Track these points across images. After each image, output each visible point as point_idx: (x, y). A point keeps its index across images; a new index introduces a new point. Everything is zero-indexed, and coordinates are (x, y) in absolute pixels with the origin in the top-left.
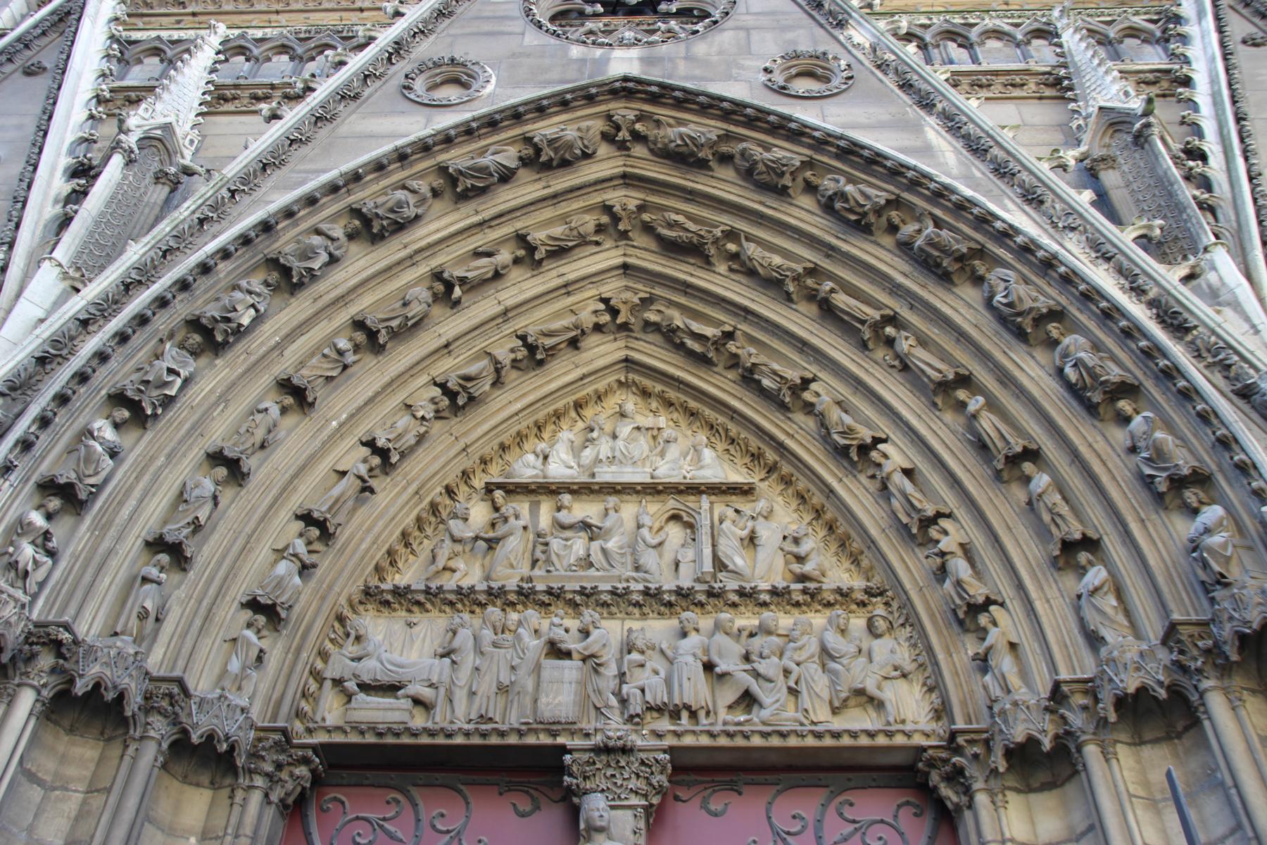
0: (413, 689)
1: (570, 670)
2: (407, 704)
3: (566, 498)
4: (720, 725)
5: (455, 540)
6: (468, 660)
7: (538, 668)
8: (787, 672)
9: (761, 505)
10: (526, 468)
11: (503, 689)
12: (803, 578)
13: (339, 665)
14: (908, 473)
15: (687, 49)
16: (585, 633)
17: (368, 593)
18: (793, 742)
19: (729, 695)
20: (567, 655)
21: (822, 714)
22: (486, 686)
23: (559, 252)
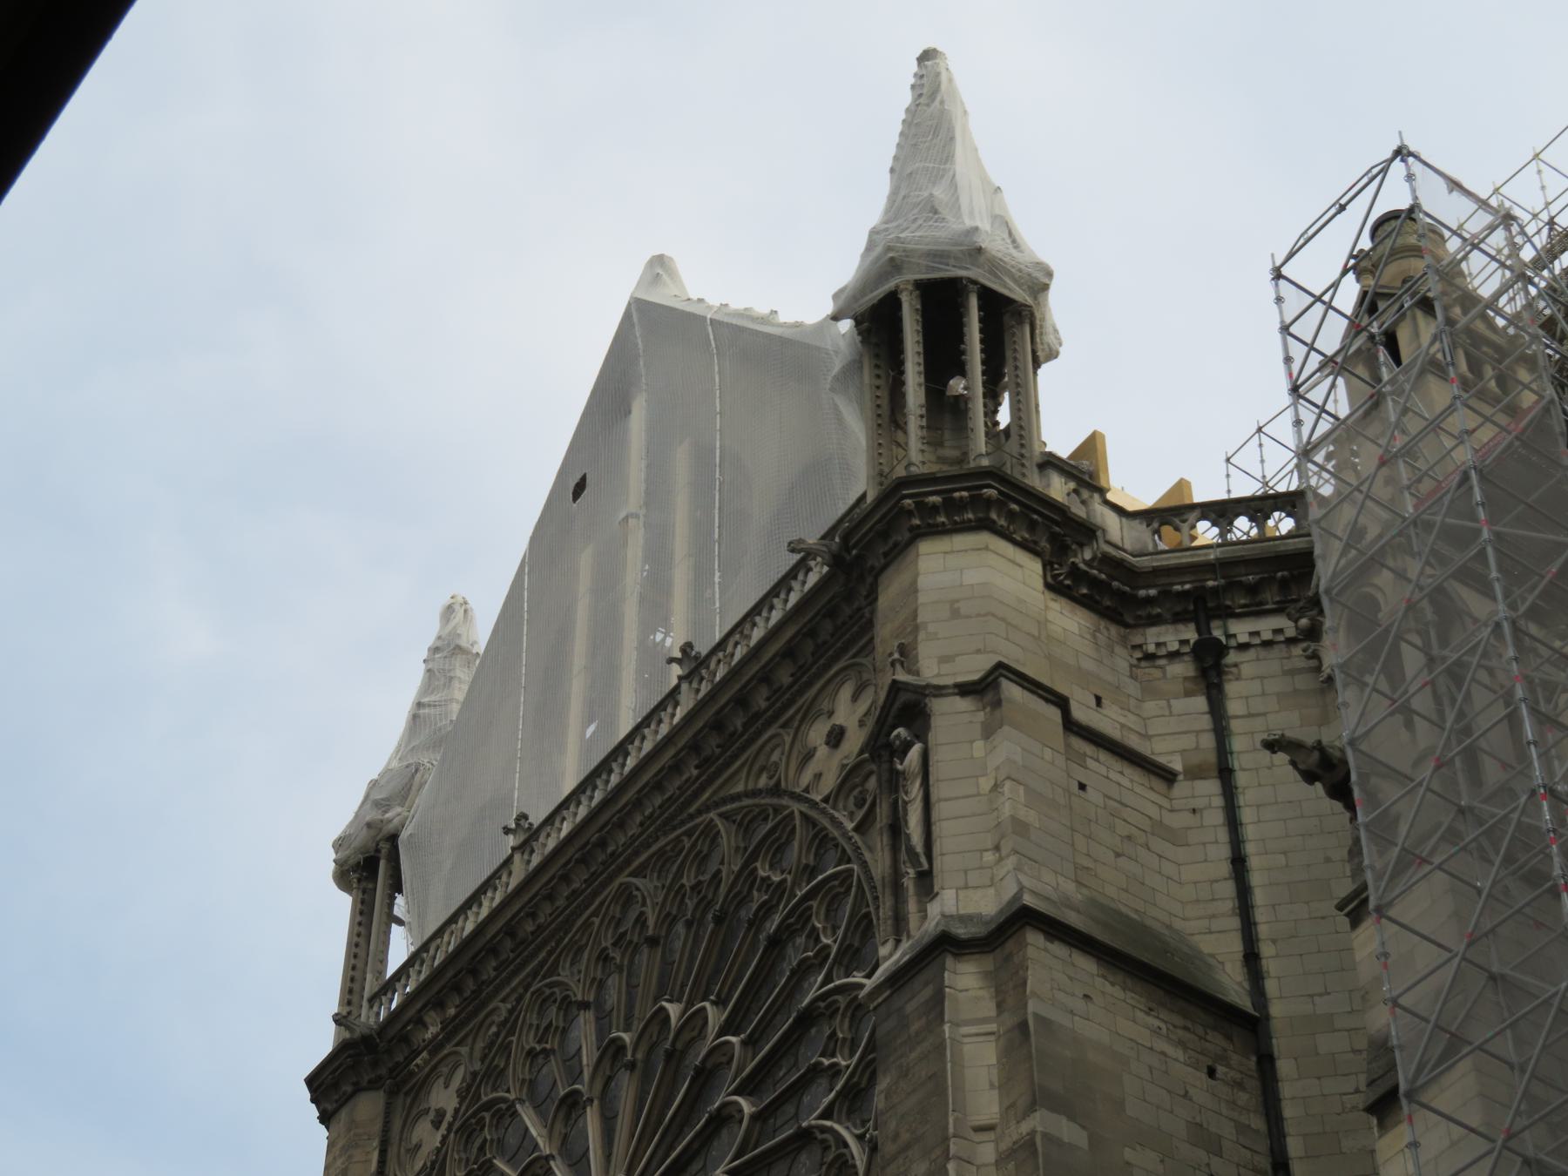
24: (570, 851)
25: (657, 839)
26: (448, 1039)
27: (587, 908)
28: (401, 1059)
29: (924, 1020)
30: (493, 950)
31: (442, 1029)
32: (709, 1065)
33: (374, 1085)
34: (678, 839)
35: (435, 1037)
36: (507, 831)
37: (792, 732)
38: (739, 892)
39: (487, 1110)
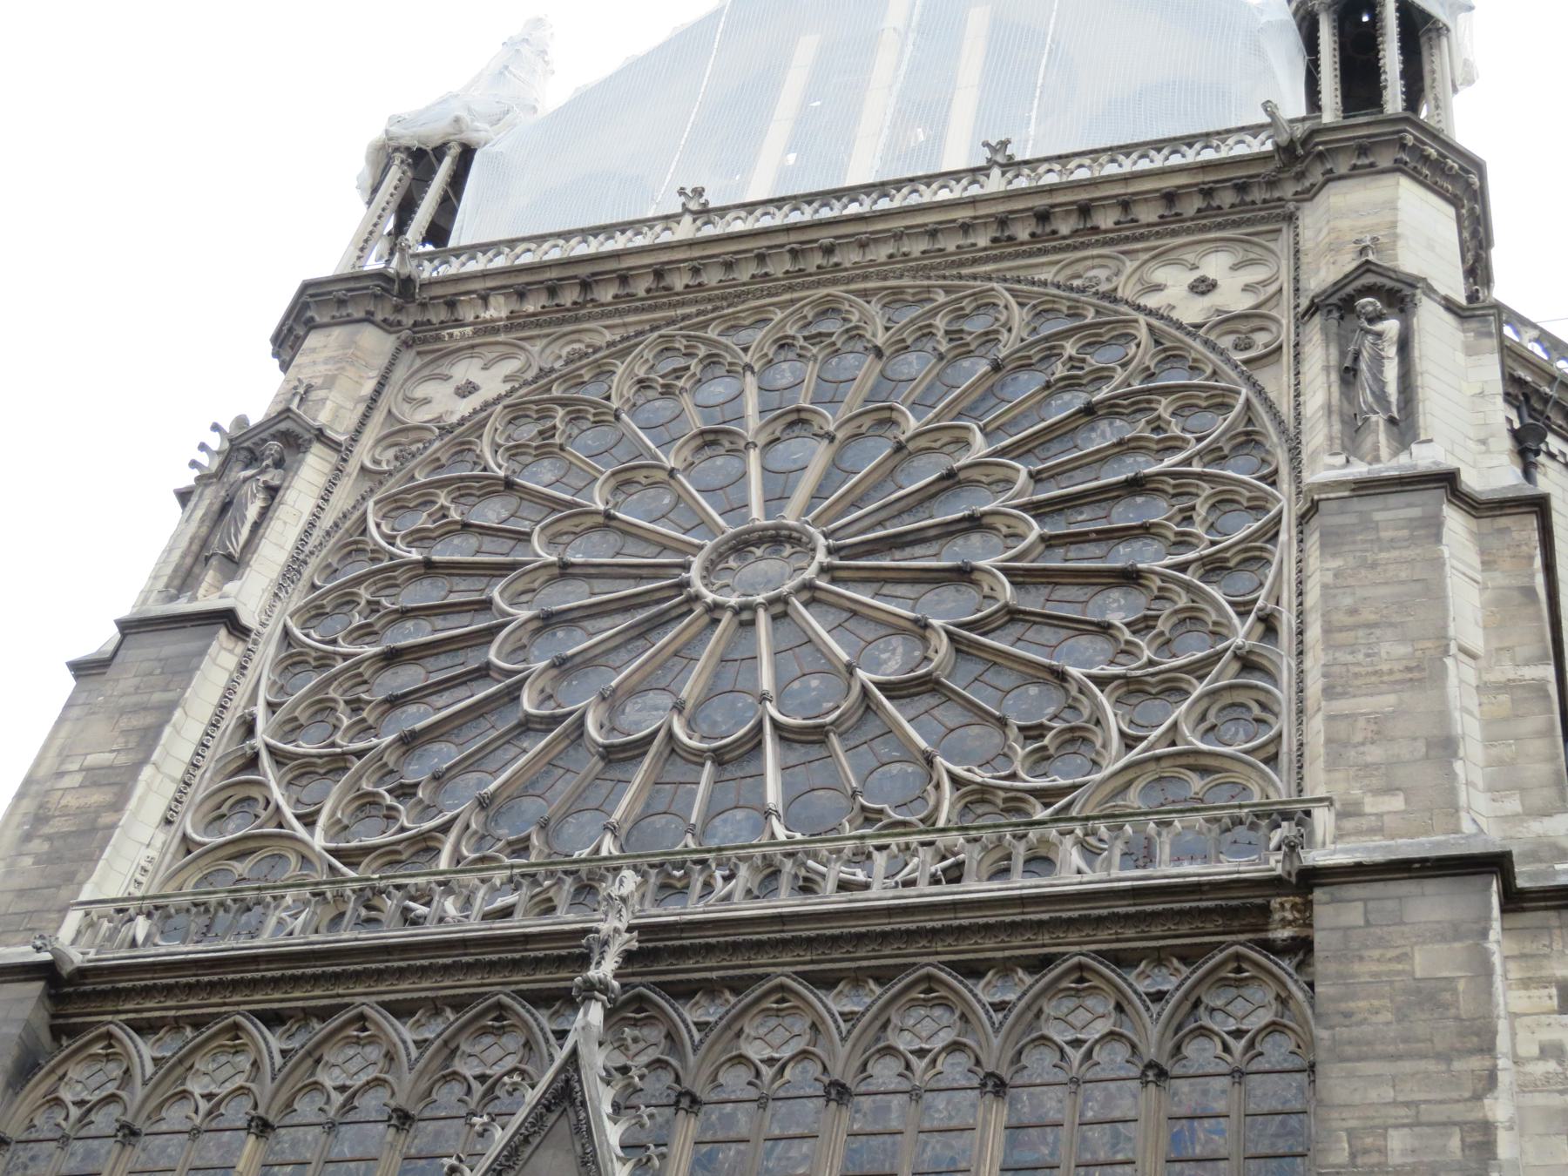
24: (795, 237)
25: (901, 277)
26: (508, 329)
27: (770, 295)
28: (434, 320)
29: (1405, 533)
30: (624, 279)
31: (508, 318)
32: (962, 476)
33: (388, 326)
34: (928, 289)
35: (493, 320)
36: (682, 192)
37: (1136, 264)
38: (1029, 357)
39: (563, 405)
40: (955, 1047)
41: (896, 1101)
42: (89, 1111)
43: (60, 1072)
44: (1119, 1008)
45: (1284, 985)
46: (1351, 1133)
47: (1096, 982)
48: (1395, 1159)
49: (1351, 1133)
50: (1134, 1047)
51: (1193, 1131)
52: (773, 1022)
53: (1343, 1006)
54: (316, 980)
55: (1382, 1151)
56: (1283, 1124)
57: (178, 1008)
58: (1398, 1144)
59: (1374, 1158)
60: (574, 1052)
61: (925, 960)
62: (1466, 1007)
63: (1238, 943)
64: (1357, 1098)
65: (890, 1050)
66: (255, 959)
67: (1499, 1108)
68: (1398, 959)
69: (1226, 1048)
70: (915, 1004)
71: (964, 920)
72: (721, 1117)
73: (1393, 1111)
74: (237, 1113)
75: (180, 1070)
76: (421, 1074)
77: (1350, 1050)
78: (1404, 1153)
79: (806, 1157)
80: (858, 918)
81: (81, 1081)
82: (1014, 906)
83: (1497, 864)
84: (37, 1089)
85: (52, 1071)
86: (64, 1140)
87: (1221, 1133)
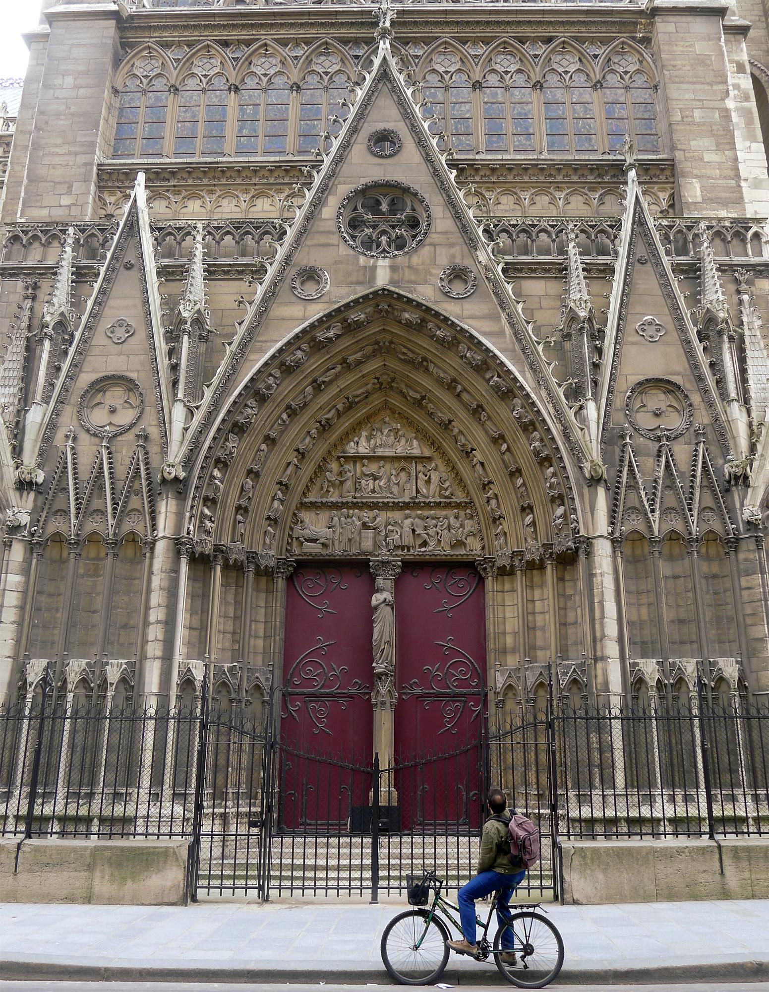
0: (321, 540)
1: (370, 533)
2: (320, 546)
3: (365, 461)
4: (418, 552)
5: (329, 481)
6: (339, 530)
7: (360, 533)
8: (438, 533)
9: (433, 465)
10: (351, 449)
11: (350, 540)
12: (446, 497)
13: (298, 531)
14: (482, 464)
15: (409, 259)
16: (375, 518)
17: (301, 503)
18: (438, 557)
19: (419, 542)
20: (369, 528)
21: (447, 548)
22: (344, 539)
23: (359, 363)
40: (519, 71)
41: (499, 91)
42: (151, 80)
43: (131, 63)
44: (580, 60)
45: (642, 55)
46: (681, 109)
47: (570, 49)
48: (697, 120)
49: (681, 109)
50: (588, 75)
51: (614, 109)
52: (443, 57)
53: (672, 63)
54: (243, 26)
55: (692, 117)
56: (646, 107)
57: (179, 37)
58: (697, 114)
59: (690, 119)
60: (385, 58)
61: (503, 35)
62: (716, 66)
63: (623, 37)
64: (681, 97)
65: (493, 71)
66: (213, 15)
67: (730, 104)
68: (691, 46)
69: (622, 78)
70: (499, 53)
71: (521, 18)
72: (430, 93)
73: (694, 103)
74: (220, 83)
75: (188, 64)
76: (300, 69)
77: (677, 79)
78: (700, 118)
79: (468, 111)
80: (477, 14)
81: (142, 67)
82: (539, 14)
83: (720, 12)
84: (124, 69)
85: (128, 62)
86: (144, 92)
87: (623, 109)
